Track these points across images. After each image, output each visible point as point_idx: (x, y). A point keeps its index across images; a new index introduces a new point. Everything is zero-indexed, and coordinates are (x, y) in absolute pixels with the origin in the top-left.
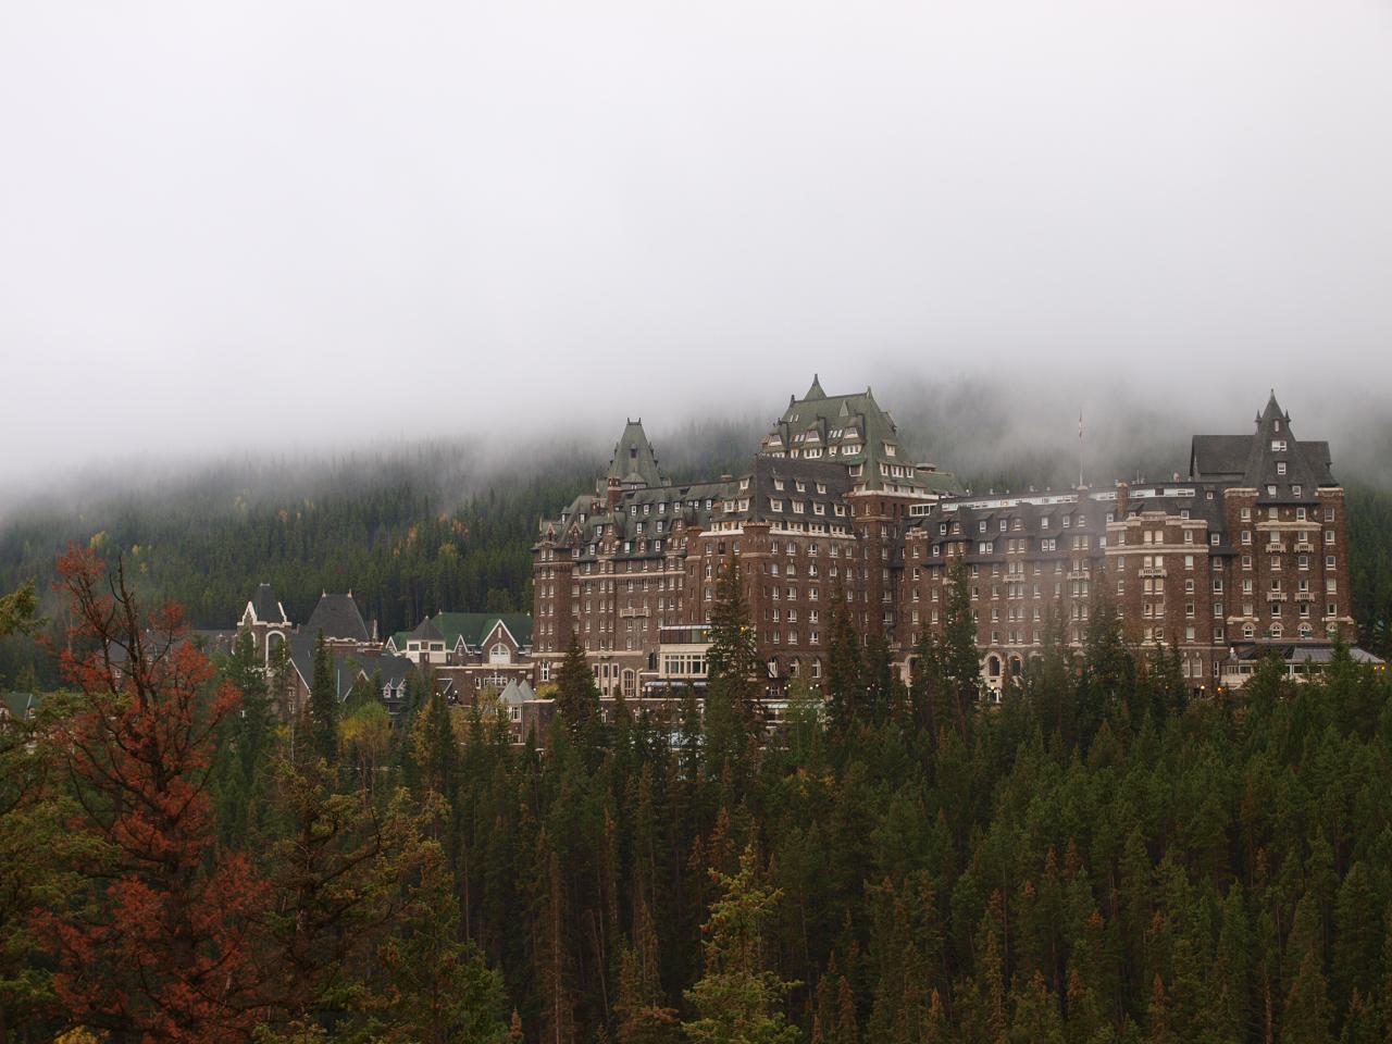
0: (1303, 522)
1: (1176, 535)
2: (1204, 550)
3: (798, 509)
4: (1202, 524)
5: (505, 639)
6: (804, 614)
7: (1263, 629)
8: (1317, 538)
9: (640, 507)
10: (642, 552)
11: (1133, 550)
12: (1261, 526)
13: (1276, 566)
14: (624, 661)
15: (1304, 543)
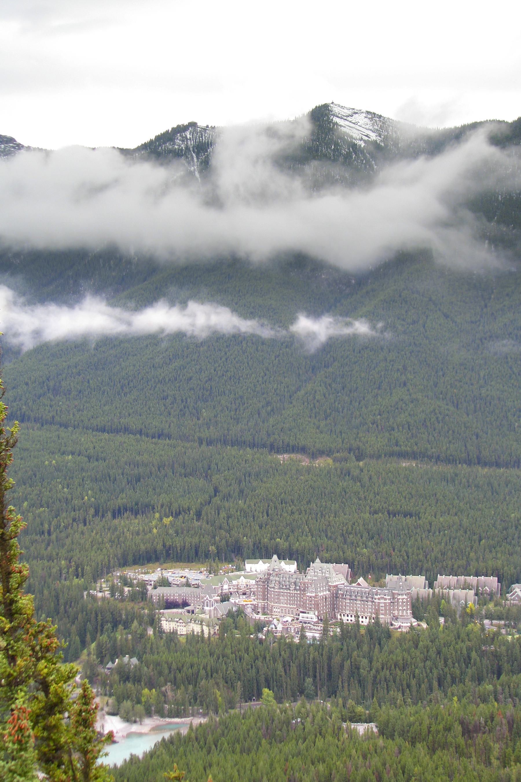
0: (405, 597)
1: (386, 599)
2: (390, 601)
3: (322, 589)
4: (389, 597)
5: (227, 582)
6: (323, 608)
7: (398, 613)
8: (407, 599)
9: (283, 578)
10: (284, 587)
11: (379, 601)
12: (398, 597)
13: (400, 604)
14: (281, 607)
15: (405, 600)
